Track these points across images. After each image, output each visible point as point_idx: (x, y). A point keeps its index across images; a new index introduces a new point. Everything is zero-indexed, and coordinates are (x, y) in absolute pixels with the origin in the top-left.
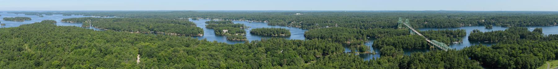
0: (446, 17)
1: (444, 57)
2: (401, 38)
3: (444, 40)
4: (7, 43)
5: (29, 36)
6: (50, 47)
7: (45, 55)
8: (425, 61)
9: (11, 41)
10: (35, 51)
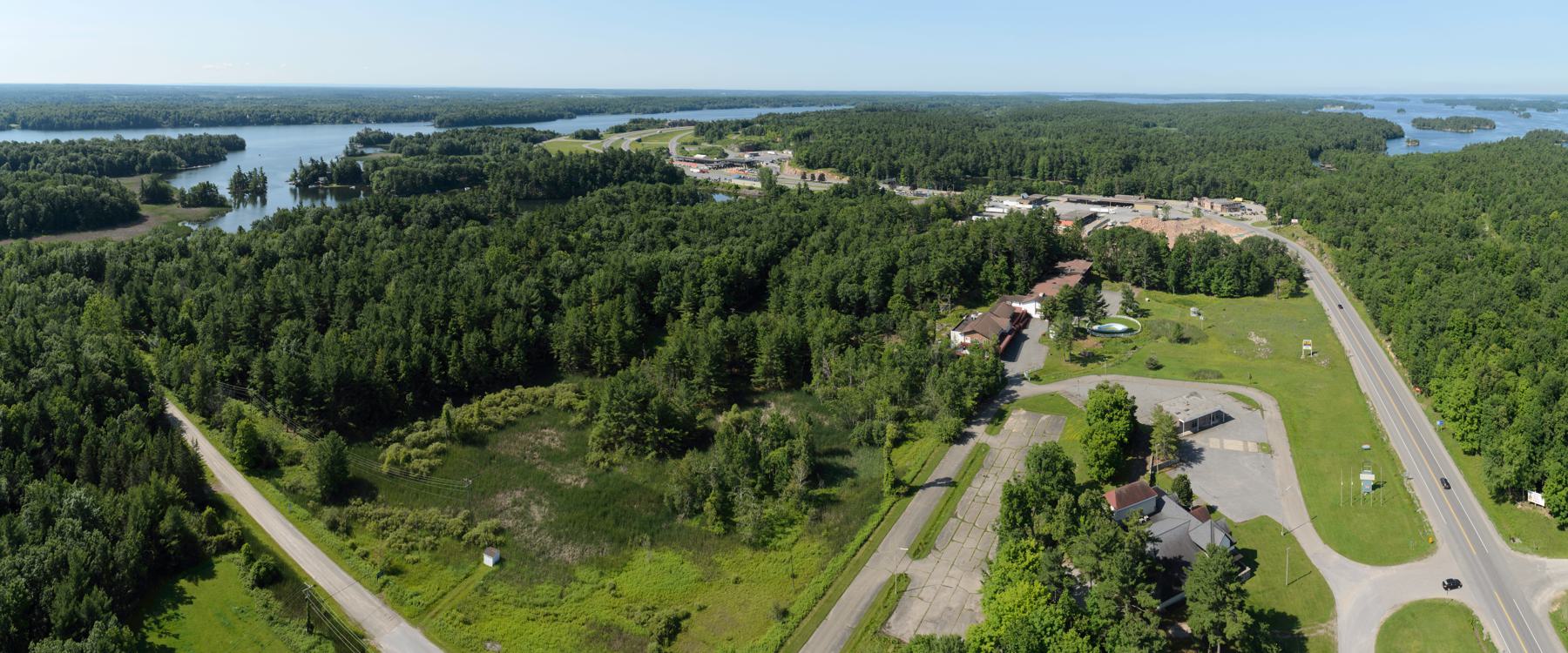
4: (1430, 209)
5: (1492, 184)
6: (1557, 229)
7: (1544, 260)
9: (1441, 200)
10: (1512, 241)
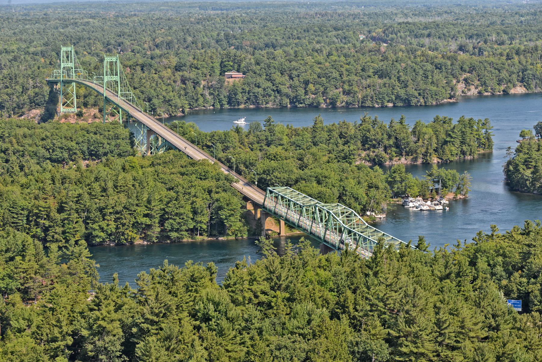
0: (362, 37)
1: (349, 293)
2: (78, 182)
3: (350, 184)
8: (231, 320)
